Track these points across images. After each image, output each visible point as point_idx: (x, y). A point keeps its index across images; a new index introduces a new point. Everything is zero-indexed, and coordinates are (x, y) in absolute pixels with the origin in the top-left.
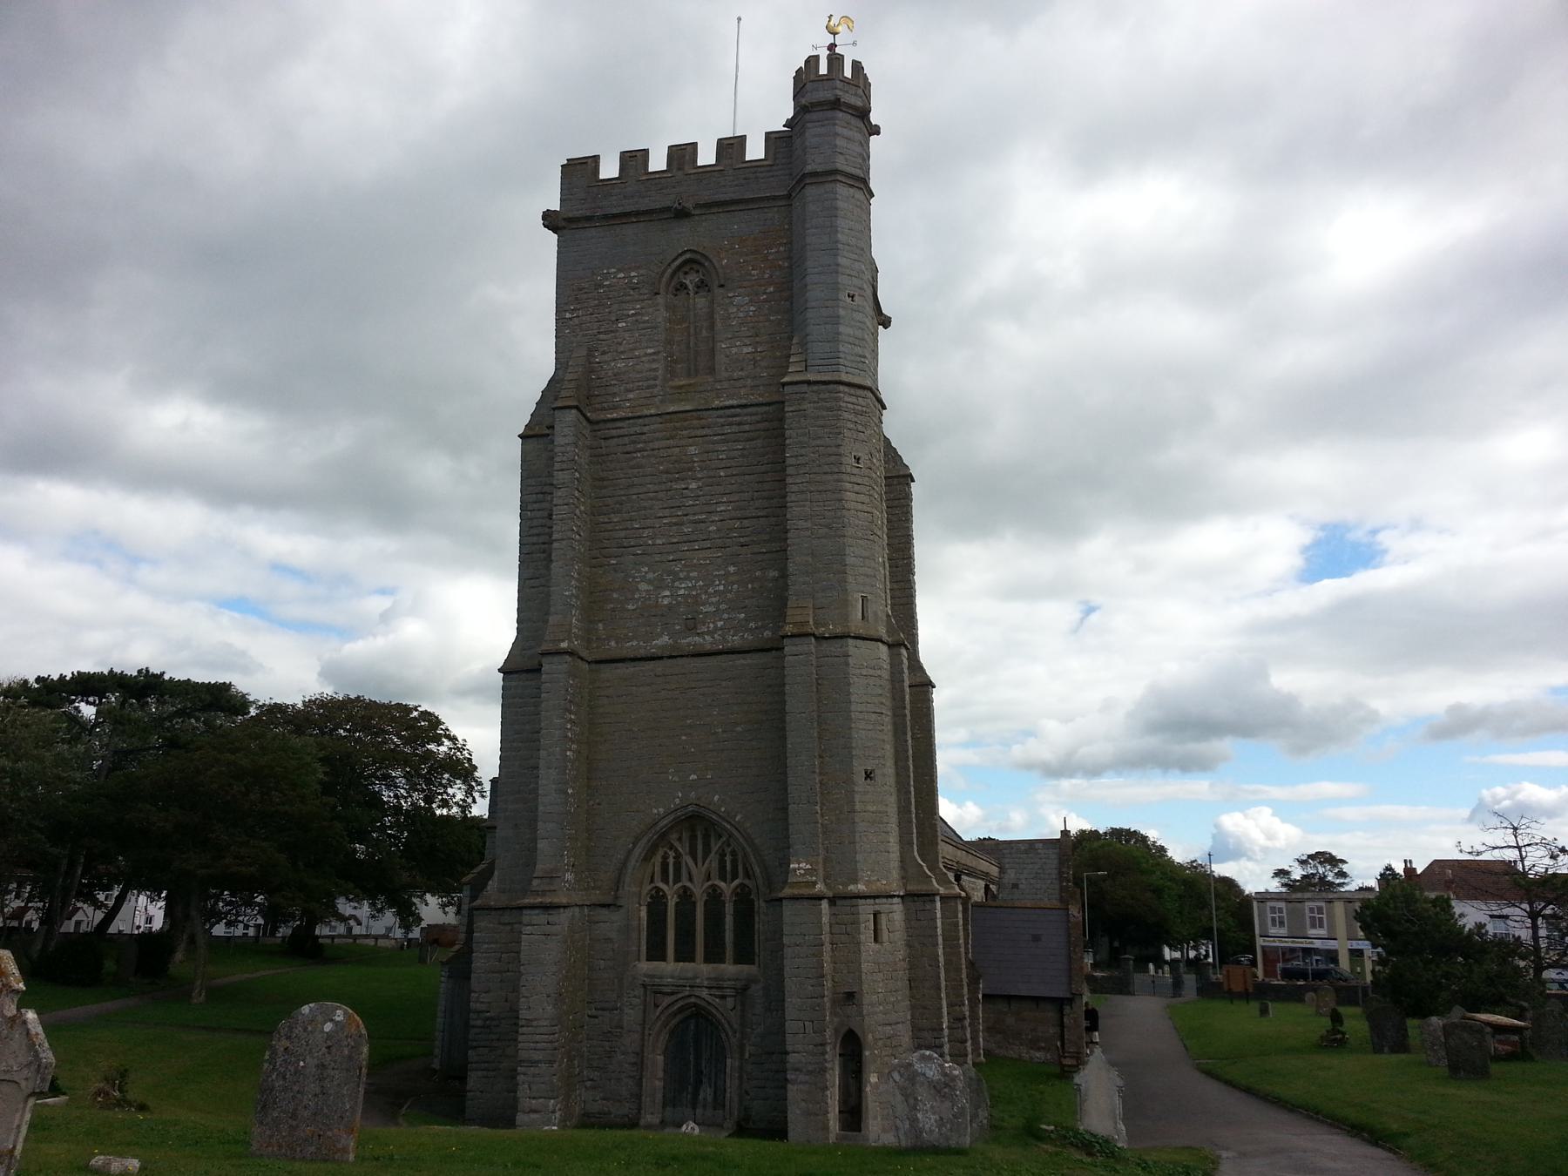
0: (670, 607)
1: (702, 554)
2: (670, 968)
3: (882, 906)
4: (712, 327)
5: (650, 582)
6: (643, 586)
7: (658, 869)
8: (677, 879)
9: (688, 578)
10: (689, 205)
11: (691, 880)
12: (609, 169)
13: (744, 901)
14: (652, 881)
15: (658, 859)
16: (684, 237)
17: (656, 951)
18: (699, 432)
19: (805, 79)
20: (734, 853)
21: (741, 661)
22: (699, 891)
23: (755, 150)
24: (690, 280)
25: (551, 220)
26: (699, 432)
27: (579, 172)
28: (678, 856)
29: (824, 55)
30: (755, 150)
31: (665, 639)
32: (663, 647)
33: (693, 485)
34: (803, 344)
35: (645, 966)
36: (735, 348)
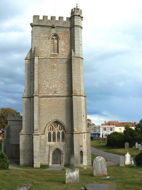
0: (52, 89)
1: (57, 81)
2: (52, 143)
4: (58, 45)
5: (48, 85)
6: (47, 86)
7: (50, 128)
8: (53, 130)
9: (55, 85)
10: (55, 26)
11: (55, 130)
12: (41, 18)
13: (63, 133)
14: (49, 130)
16: (53, 31)
17: (50, 140)
18: (56, 62)
20: (61, 127)
21: (63, 98)
22: (56, 132)
23: (65, 19)
24: (54, 37)
25: (32, 25)
26: (56, 62)
27: (36, 17)
28: (53, 127)
30: (65, 19)
31: (51, 94)
32: (51, 95)
33: (55, 70)
35: (48, 143)
36: (61, 49)
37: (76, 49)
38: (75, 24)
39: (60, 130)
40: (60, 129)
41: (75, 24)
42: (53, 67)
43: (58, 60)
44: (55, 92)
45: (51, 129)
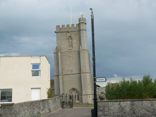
3: (90, 95)
4: (72, 43)
6: (67, 68)
8: (72, 94)
12: (61, 27)
13: (78, 96)
15: (70, 92)
16: (69, 34)
19: (80, 20)
20: (77, 92)
21: (77, 75)
24: (69, 38)
27: (58, 27)
28: (72, 92)
29: (81, 17)
30: (75, 26)
31: (69, 73)
34: (81, 46)
36: (74, 45)
37: (82, 45)
38: (81, 29)
39: (76, 94)
40: (76, 93)
41: (81, 29)
42: (70, 57)
43: (73, 52)
44: (72, 72)
45: (71, 93)
